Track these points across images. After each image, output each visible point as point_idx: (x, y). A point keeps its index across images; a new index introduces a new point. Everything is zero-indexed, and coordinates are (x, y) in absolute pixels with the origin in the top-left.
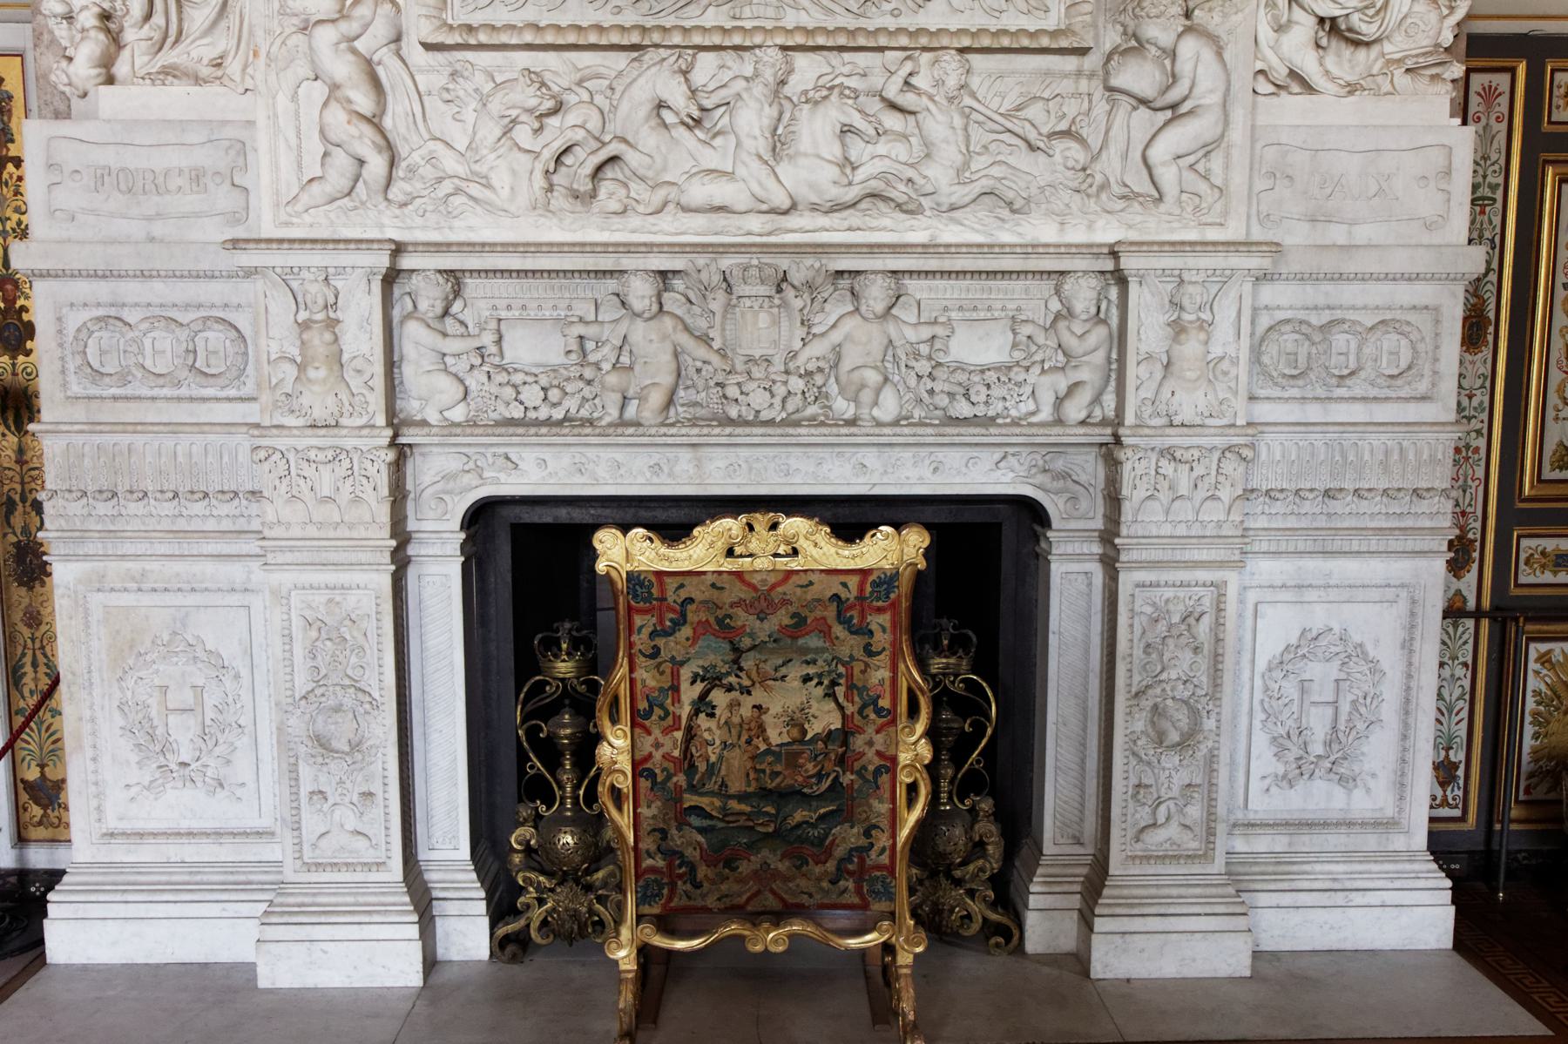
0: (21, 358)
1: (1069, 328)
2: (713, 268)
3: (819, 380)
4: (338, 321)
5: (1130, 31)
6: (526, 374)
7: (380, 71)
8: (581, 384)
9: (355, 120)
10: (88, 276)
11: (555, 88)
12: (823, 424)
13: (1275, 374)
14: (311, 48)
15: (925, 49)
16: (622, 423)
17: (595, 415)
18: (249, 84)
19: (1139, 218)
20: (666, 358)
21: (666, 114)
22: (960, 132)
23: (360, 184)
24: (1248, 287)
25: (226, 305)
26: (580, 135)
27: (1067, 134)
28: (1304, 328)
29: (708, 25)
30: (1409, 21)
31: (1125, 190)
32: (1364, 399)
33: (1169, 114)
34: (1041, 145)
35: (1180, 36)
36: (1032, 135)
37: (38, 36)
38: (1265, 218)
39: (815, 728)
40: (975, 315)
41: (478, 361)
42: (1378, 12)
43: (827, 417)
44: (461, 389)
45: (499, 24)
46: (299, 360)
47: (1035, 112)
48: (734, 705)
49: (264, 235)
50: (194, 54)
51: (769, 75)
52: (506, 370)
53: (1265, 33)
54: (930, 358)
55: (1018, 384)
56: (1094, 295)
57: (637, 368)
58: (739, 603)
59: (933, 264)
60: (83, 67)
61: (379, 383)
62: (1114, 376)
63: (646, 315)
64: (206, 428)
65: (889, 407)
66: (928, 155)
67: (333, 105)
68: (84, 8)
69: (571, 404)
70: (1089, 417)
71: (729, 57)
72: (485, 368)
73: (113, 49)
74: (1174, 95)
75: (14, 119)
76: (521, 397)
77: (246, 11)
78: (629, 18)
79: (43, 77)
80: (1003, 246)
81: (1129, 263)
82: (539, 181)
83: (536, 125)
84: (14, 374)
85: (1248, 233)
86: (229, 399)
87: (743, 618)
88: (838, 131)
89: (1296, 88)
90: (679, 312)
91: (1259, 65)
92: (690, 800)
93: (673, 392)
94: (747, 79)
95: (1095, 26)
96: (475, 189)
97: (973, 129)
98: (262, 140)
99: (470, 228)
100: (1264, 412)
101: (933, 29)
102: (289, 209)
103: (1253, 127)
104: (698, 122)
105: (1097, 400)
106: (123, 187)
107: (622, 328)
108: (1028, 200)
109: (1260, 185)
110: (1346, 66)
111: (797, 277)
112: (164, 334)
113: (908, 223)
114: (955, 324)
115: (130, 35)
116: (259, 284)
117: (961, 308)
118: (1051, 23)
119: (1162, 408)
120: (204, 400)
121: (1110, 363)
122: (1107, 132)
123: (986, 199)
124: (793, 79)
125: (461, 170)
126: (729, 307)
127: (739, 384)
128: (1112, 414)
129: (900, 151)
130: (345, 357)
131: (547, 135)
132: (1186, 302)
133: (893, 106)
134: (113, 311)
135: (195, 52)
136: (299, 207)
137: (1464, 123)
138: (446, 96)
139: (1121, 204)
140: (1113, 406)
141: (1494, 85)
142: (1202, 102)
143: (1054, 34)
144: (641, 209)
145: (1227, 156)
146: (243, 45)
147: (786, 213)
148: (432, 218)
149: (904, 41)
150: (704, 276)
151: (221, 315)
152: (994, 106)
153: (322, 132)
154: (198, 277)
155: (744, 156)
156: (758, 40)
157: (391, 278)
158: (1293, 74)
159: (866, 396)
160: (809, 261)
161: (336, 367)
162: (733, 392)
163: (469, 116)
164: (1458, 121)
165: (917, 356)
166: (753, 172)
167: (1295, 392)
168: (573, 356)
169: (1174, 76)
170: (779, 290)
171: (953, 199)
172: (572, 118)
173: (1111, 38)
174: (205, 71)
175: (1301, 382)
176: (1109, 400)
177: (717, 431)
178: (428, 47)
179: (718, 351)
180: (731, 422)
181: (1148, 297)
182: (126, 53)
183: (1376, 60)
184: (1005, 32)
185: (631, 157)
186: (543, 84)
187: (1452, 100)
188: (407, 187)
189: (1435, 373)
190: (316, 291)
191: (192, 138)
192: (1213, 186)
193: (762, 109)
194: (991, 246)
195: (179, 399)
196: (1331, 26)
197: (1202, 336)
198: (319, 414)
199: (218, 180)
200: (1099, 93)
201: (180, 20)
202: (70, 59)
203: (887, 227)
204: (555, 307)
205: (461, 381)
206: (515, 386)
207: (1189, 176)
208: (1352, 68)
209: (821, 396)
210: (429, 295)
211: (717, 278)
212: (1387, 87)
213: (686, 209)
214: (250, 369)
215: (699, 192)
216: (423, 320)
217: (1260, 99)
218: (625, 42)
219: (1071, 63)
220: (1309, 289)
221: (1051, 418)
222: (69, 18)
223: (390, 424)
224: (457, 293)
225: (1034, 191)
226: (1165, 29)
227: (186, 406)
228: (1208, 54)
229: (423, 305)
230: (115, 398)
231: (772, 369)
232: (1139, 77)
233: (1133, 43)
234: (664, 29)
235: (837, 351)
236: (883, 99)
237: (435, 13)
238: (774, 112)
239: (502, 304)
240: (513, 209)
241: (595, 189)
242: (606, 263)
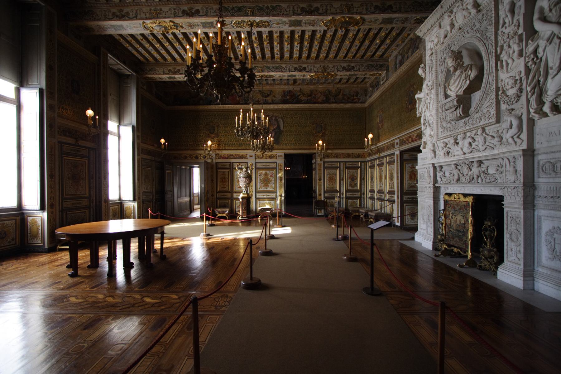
39: (462, 222)
48: (455, 218)
58: (455, 205)
87: (456, 207)
92: (451, 229)
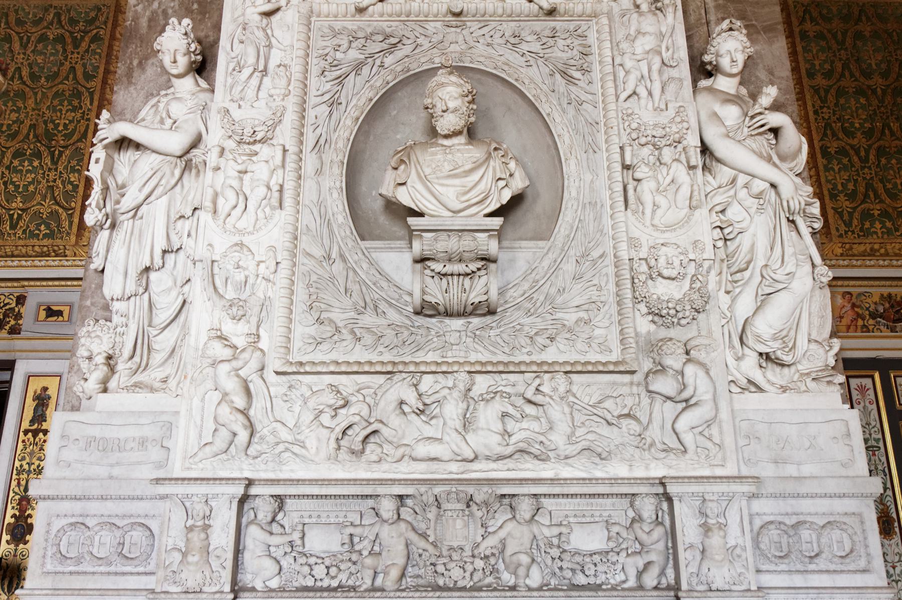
0: (21, 546)
1: (641, 528)
2: (430, 493)
3: (492, 561)
4: (210, 526)
5: (657, 361)
6: (318, 557)
7: (251, 386)
8: (350, 564)
9: (234, 412)
10: (71, 499)
11: (345, 394)
12: (495, 589)
13: (769, 556)
14: (215, 375)
15: (546, 372)
16: (373, 589)
17: (357, 583)
18: (179, 392)
19: (674, 463)
20: (401, 547)
21: (404, 407)
22: (568, 416)
23: (233, 446)
24: (744, 503)
25: (146, 516)
26: (357, 419)
27: (628, 415)
28: (782, 526)
29: (428, 361)
30: (809, 353)
31: (665, 447)
32: (828, 571)
33: (684, 404)
34: (614, 422)
35: (684, 364)
36: (609, 417)
37: (71, 367)
38: (748, 462)
40: (584, 520)
41: (289, 550)
42: (790, 350)
43: (498, 585)
44: (278, 567)
45: (316, 361)
46: (183, 550)
47: (608, 404)
49: (175, 476)
50: (152, 376)
51: (461, 386)
52: (305, 555)
53: (731, 362)
54: (559, 547)
55: (614, 564)
56: (653, 507)
57: (384, 554)
59: (557, 490)
60: (92, 384)
61: (229, 564)
62: (671, 557)
63: (390, 521)
64: (122, 592)
65: (535, 578)
66: (551, 428)
67: (224, 404)
68: (99, 353)
69: (343, 577)
70: (659, 584)
71: (440, 377)
72: (293, 554)
73: (110, 374)
74: (686, 395)
75: (49, 409)
76: (314, 573)
77: (184, 355)
78: (387, 357)
79: (69, 388)
80: (597, 479)
81: (672, 489)
82: (333, 444)
83: (333, 414)
84: (15, 556)
85: (739, 470)
86: (138, 574)
88: (500, 416)
89: (753, 389)
90: (409, 519)
91: (731, 378)
93: (405, 569)
94: (449, 388)
95: (637, 359)
96: (296, 449)
97: (575, 414)
98: (182, 422)
99: (292, 471)
100: (767, 580)
101: (550, 362)
102: (191, 460)
103: (732, 410)
104: (422, 412)
105: (662, 573)
106: (101, 448)
107: (376, 529)
108: (609, 453)
109: (741, 442)
110: (779, 376)
111: (478, 498)
112: (108, 533)
113: (541, 467)
114: (572, 525)
115: (120, 367)
116: (167, 504)
117: (575, 516)
118: (614, 357)
119: (703, 579)
120: (124, 574)
121: (668, 549)
122: (651, 415)
123: (585, 452)
124: (475, 388)
125: (290, 438)
126: (439, 517)
127: (444, 564)
128: (673, 582)
129: (535, 426)
130: (211, 548)
131: (339, 419)
132: (709, 512)
133: (530, 402)
134: (80, 520)
135: (153, 375)
136: (197, 459)
137: (852, 407)
138: (285, 398)
139: (663, 455)
140: (673, 576)
142: (702, 398)
143: (616, 364)
144: (389, 459)
145: (720, 427)
146: (179, 373)
147: (472, 461)
148: (271, 465)
149: (535, 368)
150: (424, 498)
151: (142, 521)
152: (586, 401)
153: (215, 418)
154: (133, 499)
155: (448, 430)
156: (455, 368)
157: (243, 500)
158: (750, 382)
159: (522, 571)
160: (485, 489)
161: (205, 554)
162: (441, 569)
163: (297, 409)
164: (848, 406)
165: (551, 545)
166: (453, 439)
167: (783, 567)
168: (346, 546)
169: (684, 384)
170: (468, 506)
171: (567, 453)
172: (353, 410)
173: (647, 365)
174: (157, 385)
175: (786, 561)
176: (670, 572)
177: (431, 594)
178: (277, 373)
179: (432, 543)
180: (438, 588)
181: (686, 509)
182: (116, 376)
183: (795, 374)
184: (589, 363)
185: (385, 431)
186: (338, 392)
187: (842, 395)
188: (258, 447)
189: (868, 555)
190: (200, 508)
191: (143, 421)
192: (715, 444)
193: (458, 404)
194: (590, 479)
195: (109, 573)
196: (766, 357)
197: (722, 533)
198: (191, 584)
199: (154, 443)
200: (644, 394)
201: (148, 359)
202: (86, 380)
203: (529, 469)
204: (337, 516)
205: (278, 562)
206: (310, 566)
207: (700, 439)
208: (782, 377)
209: (494, 571)
210: (264, 509)
211: (432, 499)
212: (803, 388)
213: (414, 459)
214: (154, 555)
215: (422, 450)
216: (259, 525)
217: (734, 395)
218: (384, 370)
219: (627, 378)
220: (781, 502)
221: (635, 585)
222: (90, 358)
223: (233, 590)
224: (281, 508)
225: (613, 447)
226: (676, 361)
227: (112, 578)
228: (701, 373)
229: (260, 516)
230: (71, 573)
231: (464, 554)
232: (665, 385)
233: (659, 367)
234: (405, 363)
235: (503, 542)
236: (525, 398)
237: (283, 356)
238: (465, 406)
239: (306, 514)
240: (316, 459)
241: (364, 449)
242: (368, 490)
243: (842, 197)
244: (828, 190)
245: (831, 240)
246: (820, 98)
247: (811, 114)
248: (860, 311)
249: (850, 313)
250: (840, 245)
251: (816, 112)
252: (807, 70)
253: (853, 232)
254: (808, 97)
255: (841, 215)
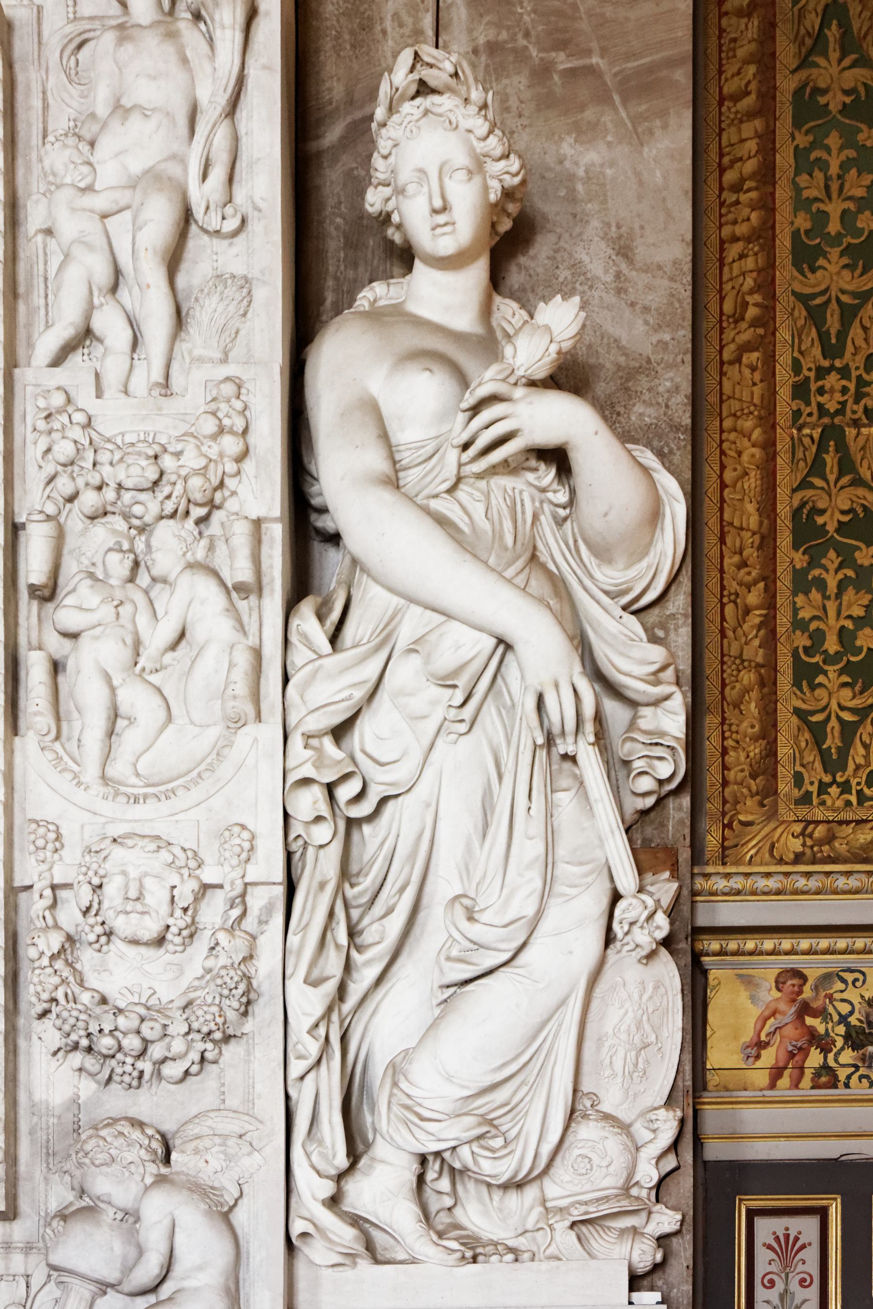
141: (793, 1234)
243: (832, 676)
244: (795, 653)
245: (773, 814)
246: (823, 337)
247: (784, 393)
248: (821, 1029)
249: (790, 1031)
250: (798, 828)
251: (800, 391)
252: (796, 235)
253: (845, 787)
254: (784, 334)
255: (818, 732)
